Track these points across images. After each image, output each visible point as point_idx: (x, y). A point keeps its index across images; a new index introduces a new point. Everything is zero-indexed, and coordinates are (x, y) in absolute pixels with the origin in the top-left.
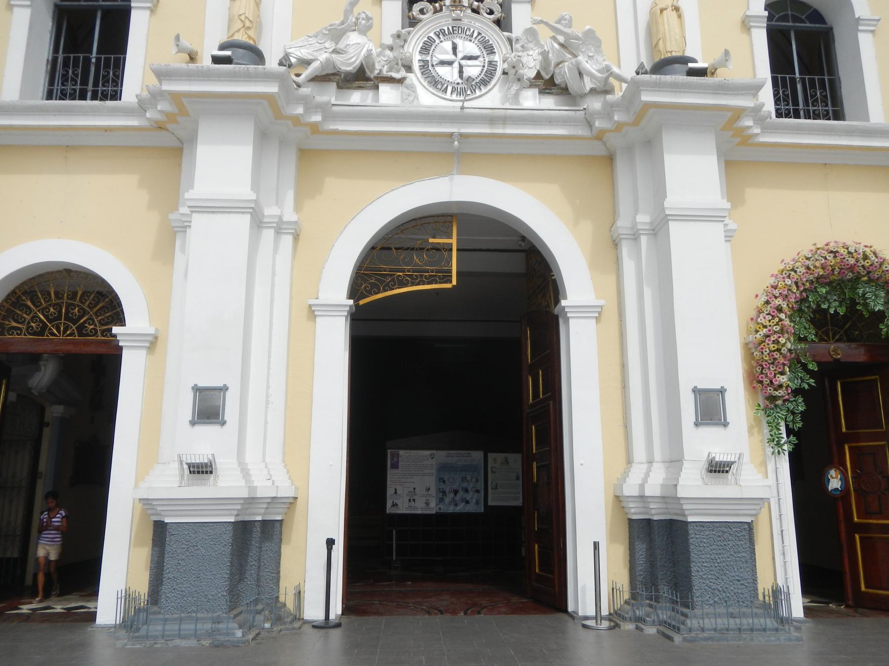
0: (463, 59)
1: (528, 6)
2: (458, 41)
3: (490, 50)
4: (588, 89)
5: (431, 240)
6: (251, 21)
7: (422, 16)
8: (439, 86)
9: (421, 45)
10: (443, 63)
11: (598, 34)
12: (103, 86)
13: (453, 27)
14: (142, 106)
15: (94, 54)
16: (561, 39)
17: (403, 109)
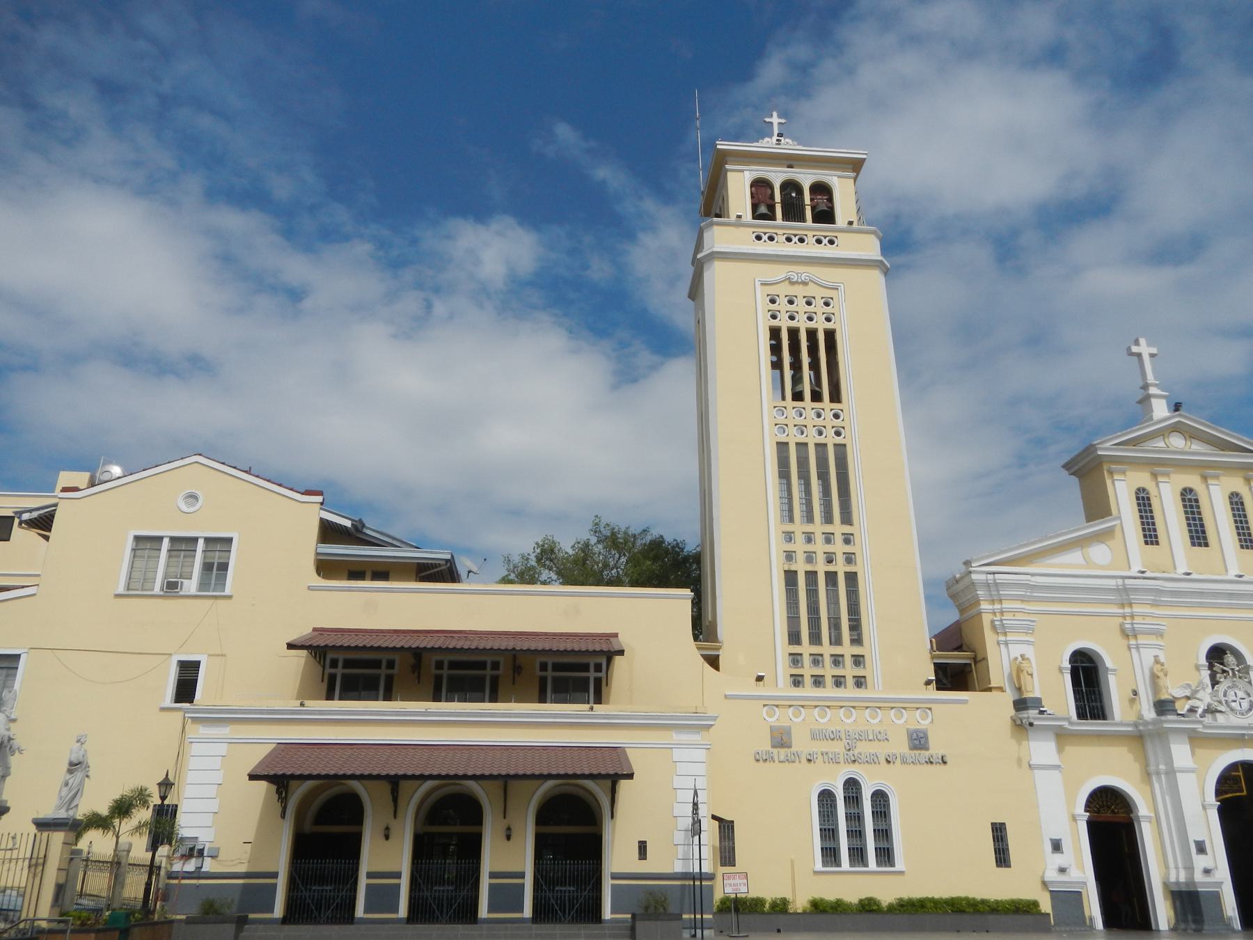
2: (1236, 691)
3: (1249, 695)
7: (1221, 680)
15: (1084, 689)
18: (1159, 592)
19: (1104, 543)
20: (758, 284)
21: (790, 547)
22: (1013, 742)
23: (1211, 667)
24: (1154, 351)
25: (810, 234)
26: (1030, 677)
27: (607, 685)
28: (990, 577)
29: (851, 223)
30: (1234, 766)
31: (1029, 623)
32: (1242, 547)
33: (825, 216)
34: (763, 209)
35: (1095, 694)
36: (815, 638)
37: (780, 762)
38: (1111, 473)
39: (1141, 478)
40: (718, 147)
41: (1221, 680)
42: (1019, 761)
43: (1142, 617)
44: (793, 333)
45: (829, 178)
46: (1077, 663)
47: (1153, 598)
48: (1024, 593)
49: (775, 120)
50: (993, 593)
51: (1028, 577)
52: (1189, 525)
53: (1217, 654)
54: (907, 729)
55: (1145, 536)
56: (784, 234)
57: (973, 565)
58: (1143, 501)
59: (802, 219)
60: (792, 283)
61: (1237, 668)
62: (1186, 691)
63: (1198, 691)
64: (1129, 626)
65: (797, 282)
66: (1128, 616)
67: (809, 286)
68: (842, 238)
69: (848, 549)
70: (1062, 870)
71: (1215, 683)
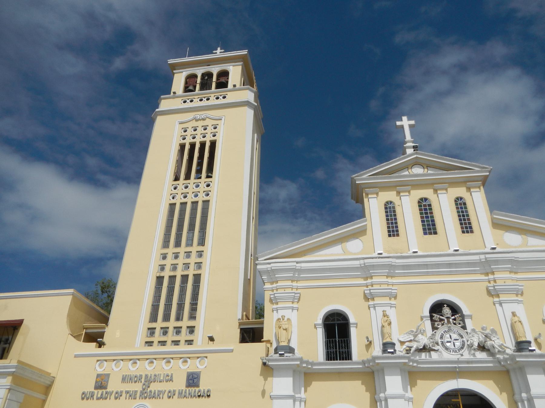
0: (454, 340)
1: (470, 319)
2: (451, 334)
3: (462, 337)
4: (497, 351)
5: (453, 400)
6: (390, 334)
7: (439, 326)
8: (448, 350)
9: (440, 336)
10: (448, 342)
11: (495, 330)
12: (342, 349)
13: (448, 329)
14: (363, 363)
15: (337, 339)
16: (485, 334)
17: (440, 360)
18: (391, 267)
19: (357, 238)
20: (177, 123)
21: (163, 262)
23: (431, 317)
24: (412, 122)
25: (212, 95)
26: (285, 331)
27: (7, 352)
28: (269, 266)
29: (235, 86)
31: (293, 294)
32: (463, 232)
33: (222, 85)
34: (191, 88)
35: (344, 342)
36: (167, 318)
37: (98, 399)
38: (367, 194)
40: (169, 62)
41: (439, 326)
42: (263, 393)
43: (379, 285)
44: (193, 146)
45: (228, 67)
46: (334, 321)
47: (388, 271)
48: (292, 275)
50: (272, 277)
51: (295, 264)
52: (423, 221)
53: (437, 308)
54: (188, 372)
55: (389, 231)
56: (198, 98)
57: (259, 260)
59: (210, 88)
60: (197, 120)
61: (453, 317)
62: (410, 336)
63: (417, 335)
64: (368, 292)
65: (200, 120)
66: (370, 285)
67: (206, 120)
69: (199, 260)
71: (434, 328)
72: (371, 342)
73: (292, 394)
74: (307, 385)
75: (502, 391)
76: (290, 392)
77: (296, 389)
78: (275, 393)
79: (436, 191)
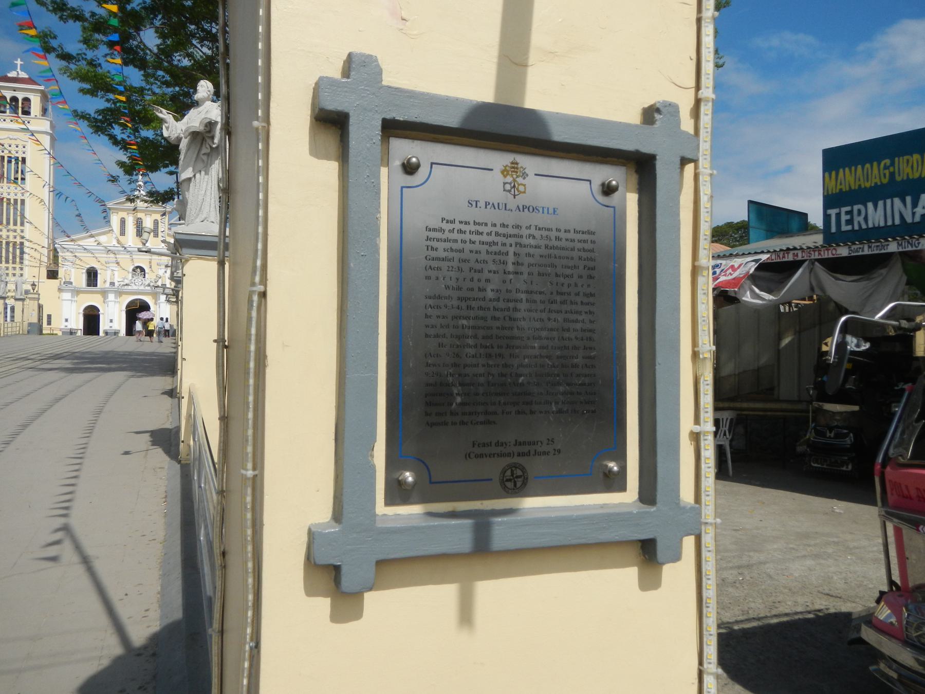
3: (142, 280)
14: (101, 289)
22: (58, 293)
29: (36, 116)
30: (137, 299)
33: (26, 112)
39: (123, 214)
42: (59, 298)
49: (19, 62)
53: (134, 270)
58: (123, 222)
60: (11, 139)
68: (32, 121)
70: (66, 326)
72: (106, 281)
73: (71, 299)
74: (77, 295)
75: (153, 299)
76: (70, 298)
77: (72, 296)
78: (64, 298)
79: (146, 215)
